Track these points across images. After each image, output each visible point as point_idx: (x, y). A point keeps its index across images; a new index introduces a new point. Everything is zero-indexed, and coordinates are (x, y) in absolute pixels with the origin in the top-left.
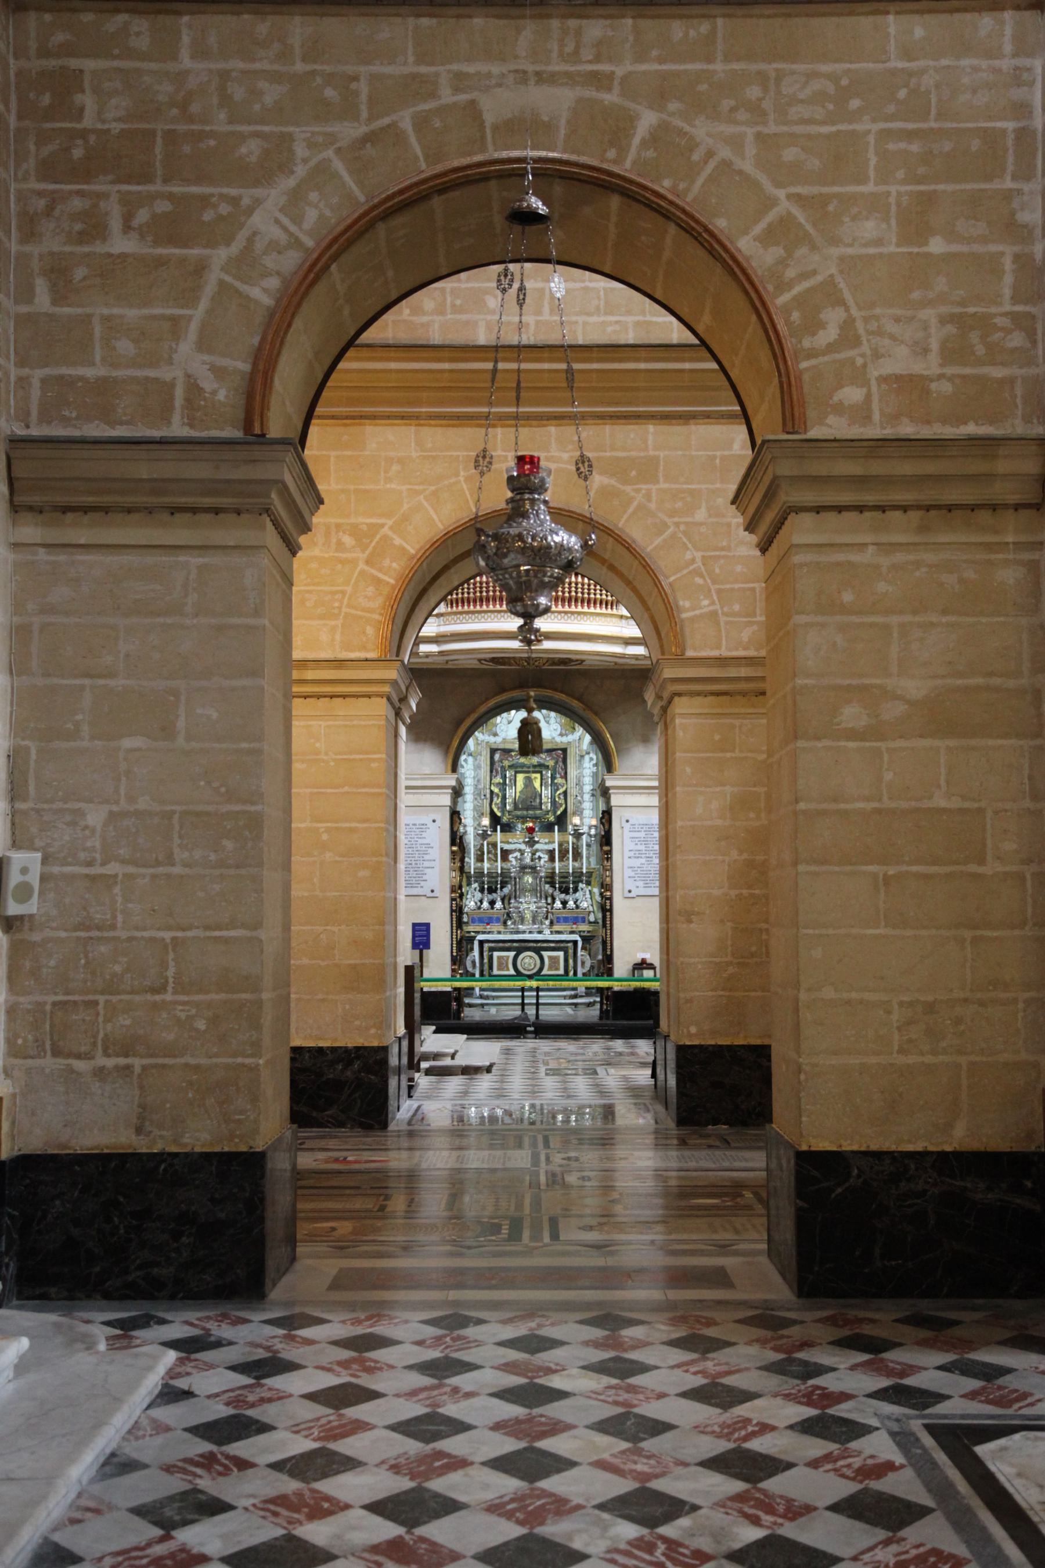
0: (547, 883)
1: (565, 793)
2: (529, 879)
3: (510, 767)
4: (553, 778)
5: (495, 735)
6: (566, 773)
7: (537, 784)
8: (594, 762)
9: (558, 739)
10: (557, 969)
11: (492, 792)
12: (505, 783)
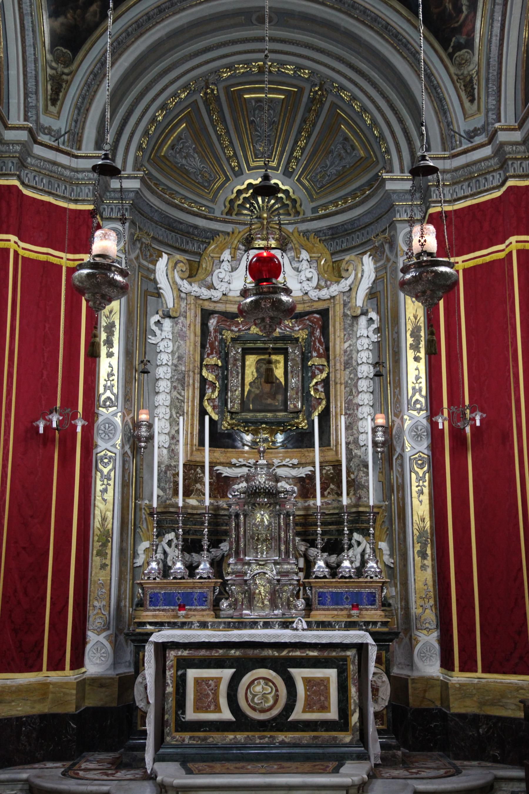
0: (298, 534)
1: (326, 382)
3: (233, 339)
4: (305, 358)
5: (211, 287)
6: (327, 349)
8: (375, 326)
9: (314, 294)
10: (325, 708)
11: (203, 381)
12: (225, 367)
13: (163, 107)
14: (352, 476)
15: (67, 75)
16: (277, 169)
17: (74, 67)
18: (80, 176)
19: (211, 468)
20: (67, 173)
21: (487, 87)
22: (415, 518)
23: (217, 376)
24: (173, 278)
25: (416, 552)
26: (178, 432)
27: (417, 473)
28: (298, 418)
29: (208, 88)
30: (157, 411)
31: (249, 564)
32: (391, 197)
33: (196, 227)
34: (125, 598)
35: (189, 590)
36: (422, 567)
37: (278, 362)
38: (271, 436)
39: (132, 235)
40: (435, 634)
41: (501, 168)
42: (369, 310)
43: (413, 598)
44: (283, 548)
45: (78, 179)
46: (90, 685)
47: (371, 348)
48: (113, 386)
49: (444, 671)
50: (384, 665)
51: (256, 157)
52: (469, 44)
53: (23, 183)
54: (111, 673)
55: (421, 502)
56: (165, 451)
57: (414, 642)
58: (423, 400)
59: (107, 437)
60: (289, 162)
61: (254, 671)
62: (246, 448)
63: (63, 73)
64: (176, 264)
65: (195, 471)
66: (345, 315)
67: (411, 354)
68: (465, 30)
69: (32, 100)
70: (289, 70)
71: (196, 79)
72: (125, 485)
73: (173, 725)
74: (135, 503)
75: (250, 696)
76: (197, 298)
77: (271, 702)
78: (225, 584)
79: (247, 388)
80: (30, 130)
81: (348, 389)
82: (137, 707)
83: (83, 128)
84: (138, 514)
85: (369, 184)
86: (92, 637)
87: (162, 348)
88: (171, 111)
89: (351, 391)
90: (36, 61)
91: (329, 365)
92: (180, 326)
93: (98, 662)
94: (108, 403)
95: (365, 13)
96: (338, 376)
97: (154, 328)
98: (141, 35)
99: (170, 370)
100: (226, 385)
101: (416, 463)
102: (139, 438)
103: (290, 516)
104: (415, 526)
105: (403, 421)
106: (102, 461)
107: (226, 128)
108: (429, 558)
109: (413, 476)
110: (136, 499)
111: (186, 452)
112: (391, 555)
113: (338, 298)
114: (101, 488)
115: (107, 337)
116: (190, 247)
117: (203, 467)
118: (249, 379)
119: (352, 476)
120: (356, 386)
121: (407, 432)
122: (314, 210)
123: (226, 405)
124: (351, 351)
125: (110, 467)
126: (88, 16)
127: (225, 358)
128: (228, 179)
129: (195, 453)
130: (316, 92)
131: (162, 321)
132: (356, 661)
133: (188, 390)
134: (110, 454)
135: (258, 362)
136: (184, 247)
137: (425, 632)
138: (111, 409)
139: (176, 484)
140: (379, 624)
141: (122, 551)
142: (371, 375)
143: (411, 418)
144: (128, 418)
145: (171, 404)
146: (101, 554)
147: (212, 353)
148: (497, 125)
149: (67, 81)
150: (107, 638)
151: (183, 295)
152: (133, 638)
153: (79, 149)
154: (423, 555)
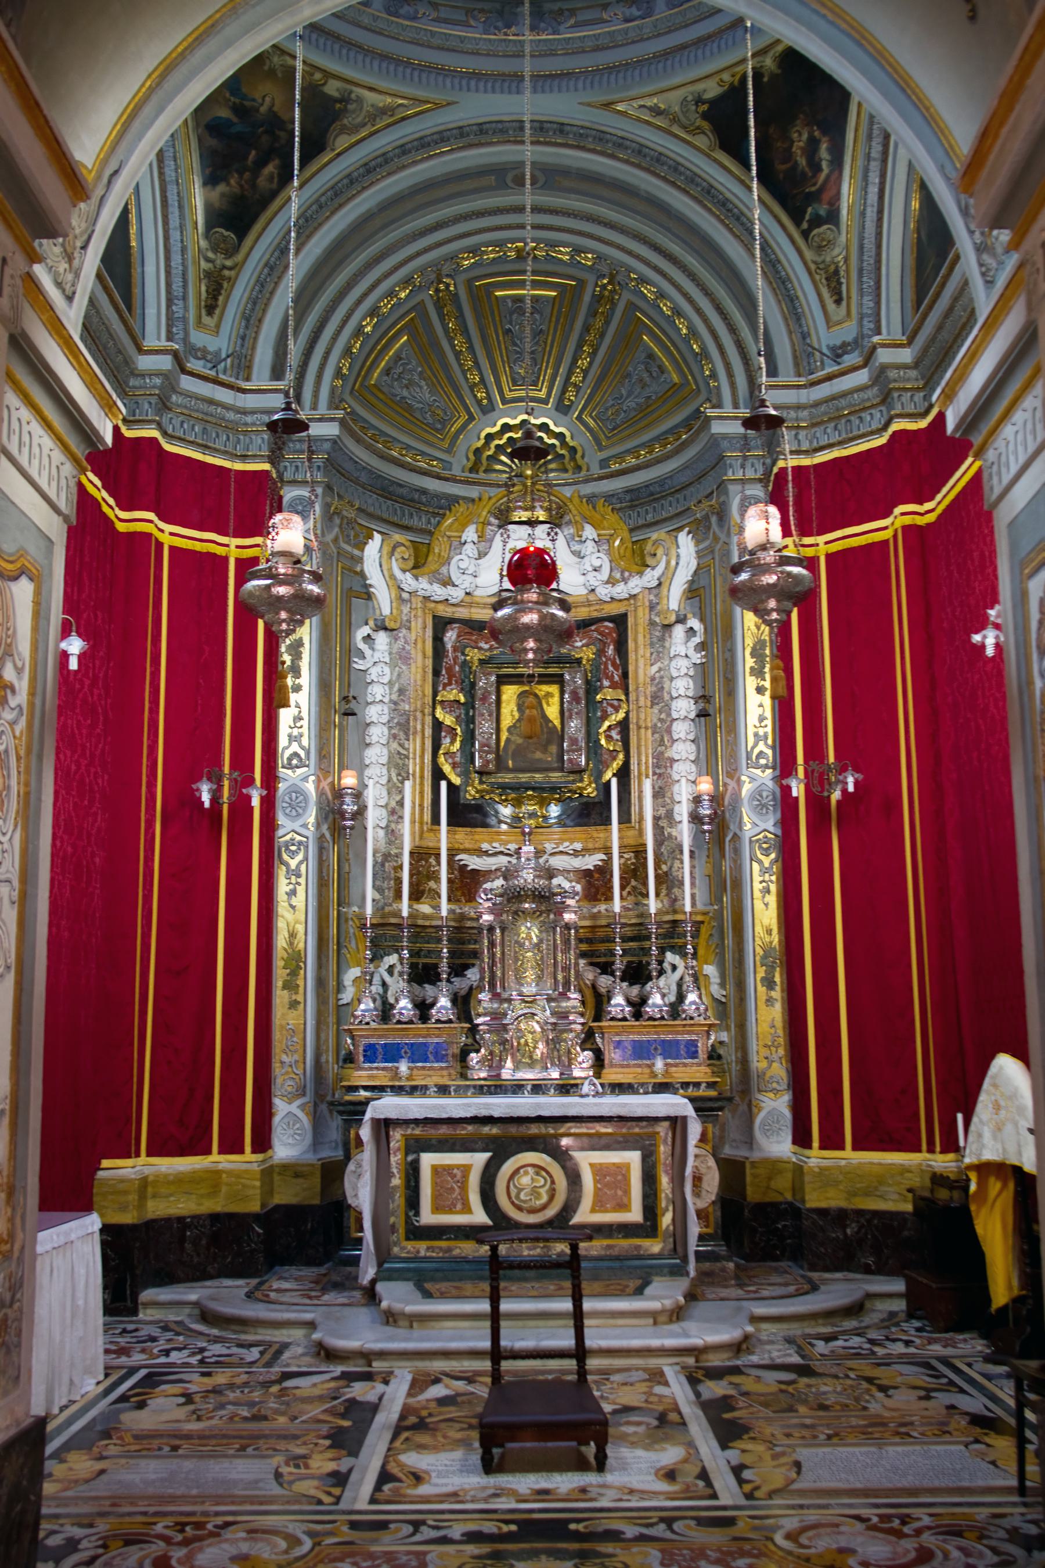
0: (583, 955)
1: (624, 726)
2: (530, 931)
4: (591, 688)
5: (447, 582)
6: (625, 675)
7: (552, 711)
8: (697, 640)
9: (604, 592)
10: (623, 1206)
11: (437, 725)
12: (470, 705)
13: (373, 312)
14: (664, 868)
15: (230, 269)
16: (545, 401)
17: (239, 257)
18: (249, 419)
19: (451, 857)
20: (231, 416)
21: (860, 282)
22: (758, 929)
23: (457, 718)
24: (390, 569)
25: (758, 979)
26: (401, 803)
27: (760, 862)
28: (581, 780)
29: (440, 282)
30: (368, 772)
31: (509, 1000)
32: (718, 445)
33: (424, 492)
34: (327, 1051)
35: (421, 1040)
36: (767, 1000)
37: (549, 695)
38: (541, 808)
39: (326, 506)
40: (786, 1098)
41: (883, 402)
42: (689, 616)
43: (753, 1046)
44: (560, 977)
45: (246, 424)
46: (280, 1174)
47: (691, 673)
48: (301, 735)
49: (797, 1149)
50: (710, 1145)
51: (515, 384)
52: (833, 217)
53: (165, 434)
54: (311, 1158)
55: (766, 905)
56: (381, 833)
57: (755, 1110)
58: (769, 752)
59: (294, 813)
60: (564, 391)
61: (520, 1156)
62: (504, 827)
63: (224, 267)
64: (394, 548)
65: (427, 861)
66: (652, 623)
67: (751, 683)
68: (826, 197)
69: (178, 308)
70: (564, 254)
71: (422, 270)
72: (322, 883)
73: (402, 1231)
74: (339, 911)
75: (513, 1192)
76: (427, 599)
77: (545, 1198)
78: (474, 1030)
79: (504, 736)
80: (175, 354)
81: (657, 736)
82: (349, 1206)
83: (254, 348)
84: (343, 926)
85: (686, 425)
86: (282, 1107)
87: (374, 677)
88: (383, 318)
89: (662, 740)
90: (184, 250)
91: (628, 700)
92: (401, 643)
93: (290, 1141)
94: (295, 762)
95: (676, 170)
96: (642, 716)
97: (361, 645)
98: (341, 206)
99: (386, 711)
100: (473, 732)
101: (760, 847)
102: (342, 814)
103: (569, 929)
104: (758, 941)
105: (739, 783)
106: (287, 849)
107: (469, 340)
108: (778, 988)
109: (755, 866)
110: (339, 905)
111: (413, 834)
112: (723, 985)
113: (640, 597)
114: (288, 889)
115: (292, 661)
116: (415, 522)
117: (438, 856)
118: (507, 721)
119: (664, 868)
120: (669, 731)
121: (745, 802)
122: (604, 463)
123: (473, 761)
124: (662, 677)
125: (300, 857)
126: (262, 181)
127: (470, 689)
128: (471, 418)
129: (426, 835)
130: (604, 287)
131: (374, 635)
132: (670, 1140)
133: (414, 740)
134: (298, 838)
135: (522, 695)
136: (406, 522)
137: (771, 1095)
138: (299, 771)
139: (399, 881)
140: (704, 1085)
141: (321, 983)
142: (692, 715)
143: (752, 779)
144: (325, 785)
145: (389, 762)
146: (290, 986)
147: (450, 684)
148: (876, 339)
149: (230, 279)
150: (302, 1107)
151: (405, 596)
152: (341, 1108)
153: (248, 379)
154: (770, 984)
